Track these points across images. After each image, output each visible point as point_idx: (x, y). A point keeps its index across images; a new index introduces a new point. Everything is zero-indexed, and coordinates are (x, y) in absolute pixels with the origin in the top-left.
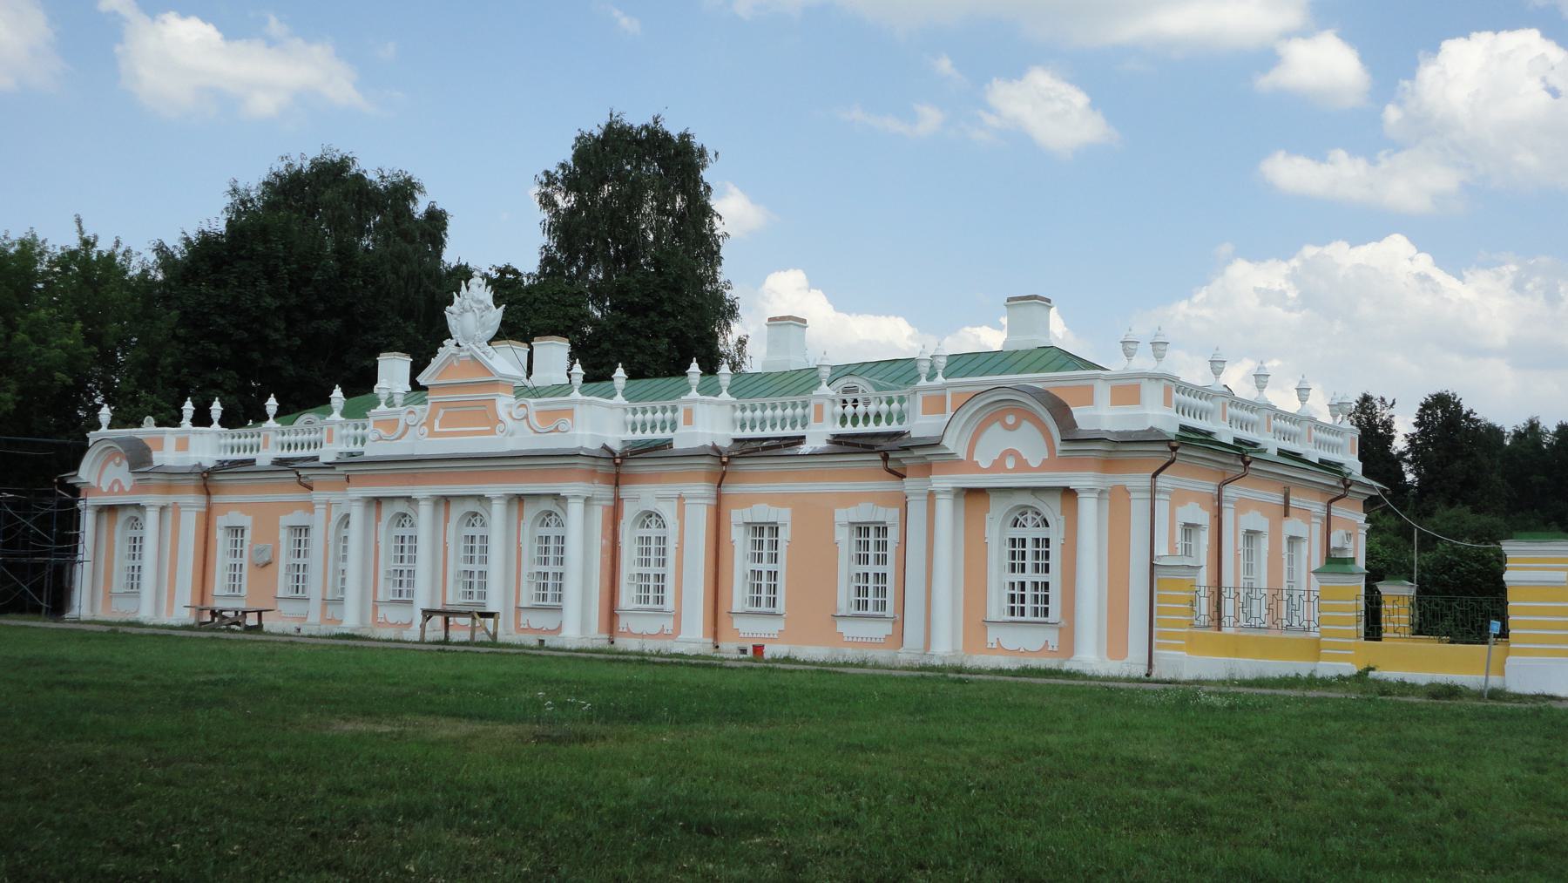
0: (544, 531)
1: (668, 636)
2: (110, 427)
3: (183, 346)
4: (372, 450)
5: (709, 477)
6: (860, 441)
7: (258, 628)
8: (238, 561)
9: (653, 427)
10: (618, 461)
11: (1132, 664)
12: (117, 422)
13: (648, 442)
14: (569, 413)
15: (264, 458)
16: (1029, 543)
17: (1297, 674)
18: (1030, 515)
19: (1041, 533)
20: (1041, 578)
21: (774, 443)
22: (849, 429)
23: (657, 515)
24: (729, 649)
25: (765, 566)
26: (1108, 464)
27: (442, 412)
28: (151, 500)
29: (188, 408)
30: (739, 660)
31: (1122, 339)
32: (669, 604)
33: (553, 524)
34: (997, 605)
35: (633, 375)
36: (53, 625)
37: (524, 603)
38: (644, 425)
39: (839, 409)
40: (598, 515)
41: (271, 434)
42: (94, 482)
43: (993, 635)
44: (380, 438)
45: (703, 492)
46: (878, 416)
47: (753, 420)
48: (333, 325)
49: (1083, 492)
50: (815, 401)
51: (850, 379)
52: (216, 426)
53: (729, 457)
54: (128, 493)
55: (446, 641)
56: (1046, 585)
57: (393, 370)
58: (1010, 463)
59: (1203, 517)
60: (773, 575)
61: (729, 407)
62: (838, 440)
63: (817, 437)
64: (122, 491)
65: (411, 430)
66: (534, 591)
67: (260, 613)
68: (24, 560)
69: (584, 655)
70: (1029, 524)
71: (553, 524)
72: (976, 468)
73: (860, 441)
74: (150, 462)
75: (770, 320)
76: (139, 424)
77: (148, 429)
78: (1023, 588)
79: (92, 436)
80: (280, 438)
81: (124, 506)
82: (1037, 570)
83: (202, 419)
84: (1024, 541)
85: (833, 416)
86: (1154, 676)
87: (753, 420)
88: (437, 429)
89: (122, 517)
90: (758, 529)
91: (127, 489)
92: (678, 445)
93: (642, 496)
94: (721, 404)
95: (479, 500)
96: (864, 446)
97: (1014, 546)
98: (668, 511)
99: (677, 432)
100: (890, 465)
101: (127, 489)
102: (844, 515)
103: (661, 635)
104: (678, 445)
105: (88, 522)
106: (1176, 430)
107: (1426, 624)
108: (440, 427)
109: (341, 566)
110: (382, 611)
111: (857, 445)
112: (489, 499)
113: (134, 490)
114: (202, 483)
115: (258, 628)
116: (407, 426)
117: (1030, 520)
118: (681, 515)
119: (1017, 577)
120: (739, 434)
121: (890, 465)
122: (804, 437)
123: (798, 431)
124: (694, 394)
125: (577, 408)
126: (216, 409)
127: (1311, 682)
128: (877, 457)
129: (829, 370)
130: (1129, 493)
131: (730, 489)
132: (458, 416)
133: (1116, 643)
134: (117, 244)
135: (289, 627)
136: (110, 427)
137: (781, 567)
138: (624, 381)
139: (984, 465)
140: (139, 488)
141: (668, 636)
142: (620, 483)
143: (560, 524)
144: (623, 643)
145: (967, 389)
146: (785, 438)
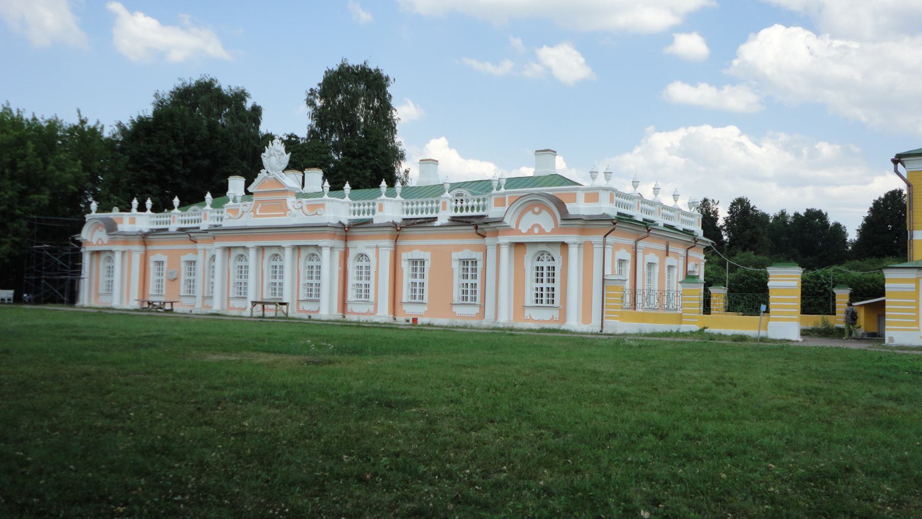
0: (311, 263)
1: (371, 314)
2: (97, 212)
3: (131, 173)
4: (226, 224)
5: (391, 237)
6: (464, 220)
7: (171, 311)
8: (160, 278)
9: (364, 213)
10: (347, 229)
11: (594, 326)
12: (100, 209)
13: (361, 220)
14: (323, 206)
15: (173, 227)
16: (545, 269)
17: (671, 331)
18: (545, 255)
19: (551, 264)
20: (551, 285)
21: (423, 220)
22: (459, 214)
23: (366, 255)
24: (401, 320)
25: (418, 280)
26: (583, 231)
27: (260, 205)
28: (117, 248)
29: (135, 203)
30: (406, 325)
31: (590, 170)
32: (372, 298)
33: (315, 260)
34: (530, 299)
35: (354, 187)
36: (70, 309)
37: (301, 298)
38: (359, 212)
39: (454, 204)
40: (337, 255)
41: (176, 216)
42: (89, 239)
43: (528, 313)
44: (230, 218)
46: (473, 208)
47: (412, 209)
48: (206, 162)
49: (571, 244)
51: (460, 190)
52: (149, 212)
53: (401, 227)
54: (105, 245)
55: (263, 317)
56: (553, 289)
57: (236, 184)
58: (536, 230)
59: (628, 256)
60: (422, 284)
61: (400, 203)
62: (453, 219)
63: (443, 218)
64: (103, 244)
65: (245, 215)
66: (306, 292)
67: (172, 303)
68: (55, 277)
69: (330, 323)
70: (545, 260)
71: (315, 260)
72: (520, 233)
73: (464, 220)
74: (116, 229)
75: (420, 161)
76: (110, 211)
77: (115, 213)
78: (542, 290)
79: (88, 216)
80: (180, 218)
81: (104, 251)
82: (549, 282)
83: (142, 208)
84: (542, 268)
85: (451, 207)
86: (604, 332)
88: (258, 213)
89: (103, 257)
90: (414, 262)
91: (105, 242)
92: (376, 222)
93: (358, 246)
94: (396, 201)
96: (466, 222)
97: (538, 270)
98: (371, 254)
99: (375, 215)
100: (479, 231)
101: (105, 242)
102: (456, 255)
103: (368, 313)
104: (376, 222)
105: (86, 259)
106: (615, 214)
107: (732, 307)
109: (212, 280)
110: (232, 302)
111: (462, 222)
112: (284, 248)
113: (109, 243)
114: (142, 240)
115: (171, 311)
116: (243, 212)
117: (545, 257)
118: (377, 256)
119: (539, 285)
120: (405, 216)
121: (479, 231)
122: (437, 218)
123: (434, 215)
124: (383, 197)
125: (327, 203)
126: (149, 203)
127: (678, 334)
128: (473, 227)
129: (449, 185)
130: (593, 245)
131: (401, 243)
132: (267, 207)
133: (586, 316)
134: (98, 123)
135: (186, 310)
136: (97, 212)
137: (426, 281)
138: (349, 190)
139: (524, 231)
140: (112, 242)
141: (371, 314)
142: (348, 239)
143: (319, 260)
144: (349, 317)
145: (516, 195)
146: (428, 218)
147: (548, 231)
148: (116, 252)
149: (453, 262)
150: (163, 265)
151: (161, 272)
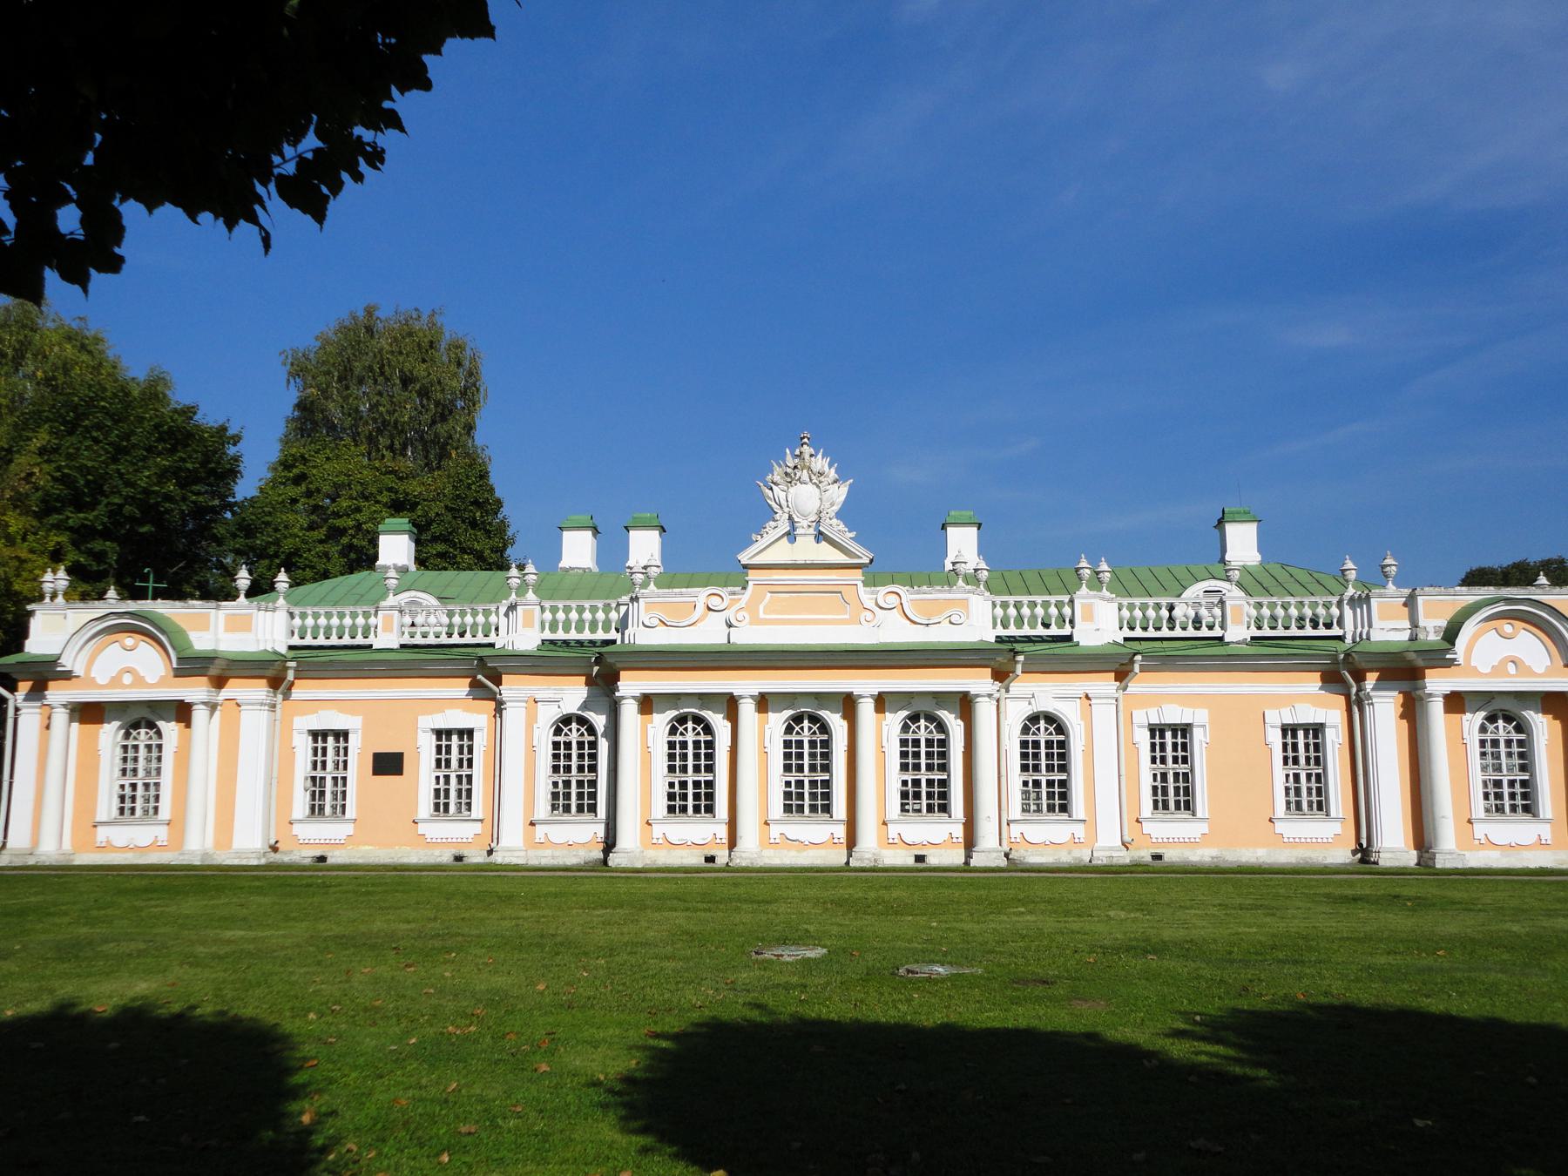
4: (643, 636)
8: (319, 773)
29: (243, 579)
32: (165, 811)
45: (264, 697)
50: (1231, 603)
72: (1475, 672)
83: (261, 588)
86: (853, 863)
87: (475, 625)
88: (762, 615)
90: (1156, 730)
95: (816, 698)
98: (1070, 713)
108: (765, 613)
138: (287, 585)
139: (101, 681)
148: (195, 707)
149: (1270, 730)
150: (346, 740)
151: (342, 758)
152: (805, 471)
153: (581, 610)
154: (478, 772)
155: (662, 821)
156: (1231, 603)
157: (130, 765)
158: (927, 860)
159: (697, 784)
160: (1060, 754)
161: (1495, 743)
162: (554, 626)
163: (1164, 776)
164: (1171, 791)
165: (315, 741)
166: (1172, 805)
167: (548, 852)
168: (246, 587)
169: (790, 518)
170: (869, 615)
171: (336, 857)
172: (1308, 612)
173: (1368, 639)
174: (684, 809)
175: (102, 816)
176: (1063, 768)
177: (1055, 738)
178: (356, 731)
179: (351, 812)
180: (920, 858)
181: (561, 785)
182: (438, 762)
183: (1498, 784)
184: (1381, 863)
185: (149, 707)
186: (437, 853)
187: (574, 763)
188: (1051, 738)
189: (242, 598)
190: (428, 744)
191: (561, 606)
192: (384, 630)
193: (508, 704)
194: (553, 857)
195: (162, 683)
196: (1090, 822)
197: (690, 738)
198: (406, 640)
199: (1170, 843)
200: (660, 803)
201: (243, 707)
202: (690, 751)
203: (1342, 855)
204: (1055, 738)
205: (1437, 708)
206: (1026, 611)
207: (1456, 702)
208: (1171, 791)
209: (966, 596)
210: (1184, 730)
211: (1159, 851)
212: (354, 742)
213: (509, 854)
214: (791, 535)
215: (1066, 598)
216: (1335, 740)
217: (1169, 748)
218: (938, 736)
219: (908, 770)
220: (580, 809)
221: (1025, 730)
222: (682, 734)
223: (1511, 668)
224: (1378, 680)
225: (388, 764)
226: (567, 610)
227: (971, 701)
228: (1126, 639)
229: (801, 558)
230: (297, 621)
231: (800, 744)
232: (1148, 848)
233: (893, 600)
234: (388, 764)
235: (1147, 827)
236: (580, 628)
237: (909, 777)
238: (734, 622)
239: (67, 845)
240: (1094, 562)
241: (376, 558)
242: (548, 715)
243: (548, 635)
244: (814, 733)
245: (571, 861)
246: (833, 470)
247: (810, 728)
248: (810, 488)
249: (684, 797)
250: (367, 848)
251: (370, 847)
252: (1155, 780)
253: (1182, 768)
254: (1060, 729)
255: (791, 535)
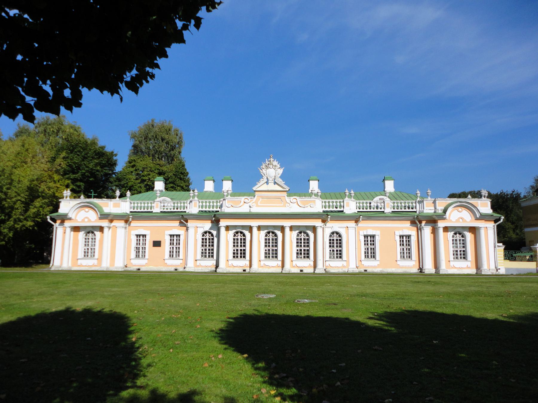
4: (227, 209)
8: (138, 246)
29: (118, 193)
32: (96, 256)
47: (181, 206)
50: (387, 202)
72: (451, 221)
83: (122, 196)
86: (283, 272)
87: (181, 206)
88: (259, 204)
90: (366, 236)
96: (407, 214)
98: (342, 232)
102: (399, 233)
103: (343, 266)
138: (130, 195)
147: (92, 220)
148: (105, 228)
149: (396, 237)
150: (146, 237)
151: (144, 242)
152: (271, 165)
153: (210, 202)
154: (181, 246)
155: (231, 260)
156: (387, 202)
157: (87, 243)
158: (303, 271)
159: (241, 250)
160: (340, 242)
161: (456, 240)
162: (202, 207)
163: (368, 249)
164: (370, 253)
165: (137, 237)
166: (370, 256)
167: (200, 268)
168: (119, 195)
169: (267, 178)
170: (288, 205)
171: (143, 269)
172: (407, 205)
173: (423, 212)
174: (237, 257)
175: (79, 257)
176: (340, 247)
177: (339, 238)
178: (148, 235)
179: (147, 257)
180: (301, 271)
181: (204, 250)
182: (171, 243)
183: (457, 251)
184: (426, 272)
185: (92, 228)
186: (170, 268)
187: (208, 244)
188: (337, 238)
189: (117, 198)
190: (168, 238)
191: (204, 201)
192: (156, 207)
193: (190, 228)
194: (202, 270)
195: (96, 221)
196: (348, 261)
197: (239, 238)
198: (162, 210)
199: (369, 267)
200: (231, 255)
201: (118, 228)
202: (239, 241)
203: (415, 270)
204: (339, 238)
205: (441, 231)
206: (331, 204)
207: (446, 229)
208: (370, 253)
209: (315, 200)
210: (373, 236)
211: (366, 269)
212: (148, 238)
213: (190, 269)
214: (267, 183)
215: (342, 200)
216: (414, 239)
217: (369, 241)
218: (307, 238)
219: (298, 247)
220: (209, 256)
221: (330, 236)
222: (237, 236)
223: (461, 220)
224: (426, 223)
225: (157, 244)
226: (206, 202)
227: (316, 228)
228: (358, 212)
229: (270, 189)
230: (132, 205)
231: (269, 239)
232: (363, 268)
233: (295, 200)
234: (157, 244)
235: (363, 263)
236: (209, 208)
237: (299, 249)
238: (251, 206)
239: (70, 265)
240: (350, 191)
241: (154, 188)
242: (201, 231)
243: (201, 209)
244: (273, 236)
245: (207, 270)
246: (279, 165)
247: (272, 235)
248: (273, 170)
249: (237, 254)
250: (151, 266)
251: (152, 266)
252: (365, 250)
253: (373, 247)
254: (340, 236)
255: (267, 183)
